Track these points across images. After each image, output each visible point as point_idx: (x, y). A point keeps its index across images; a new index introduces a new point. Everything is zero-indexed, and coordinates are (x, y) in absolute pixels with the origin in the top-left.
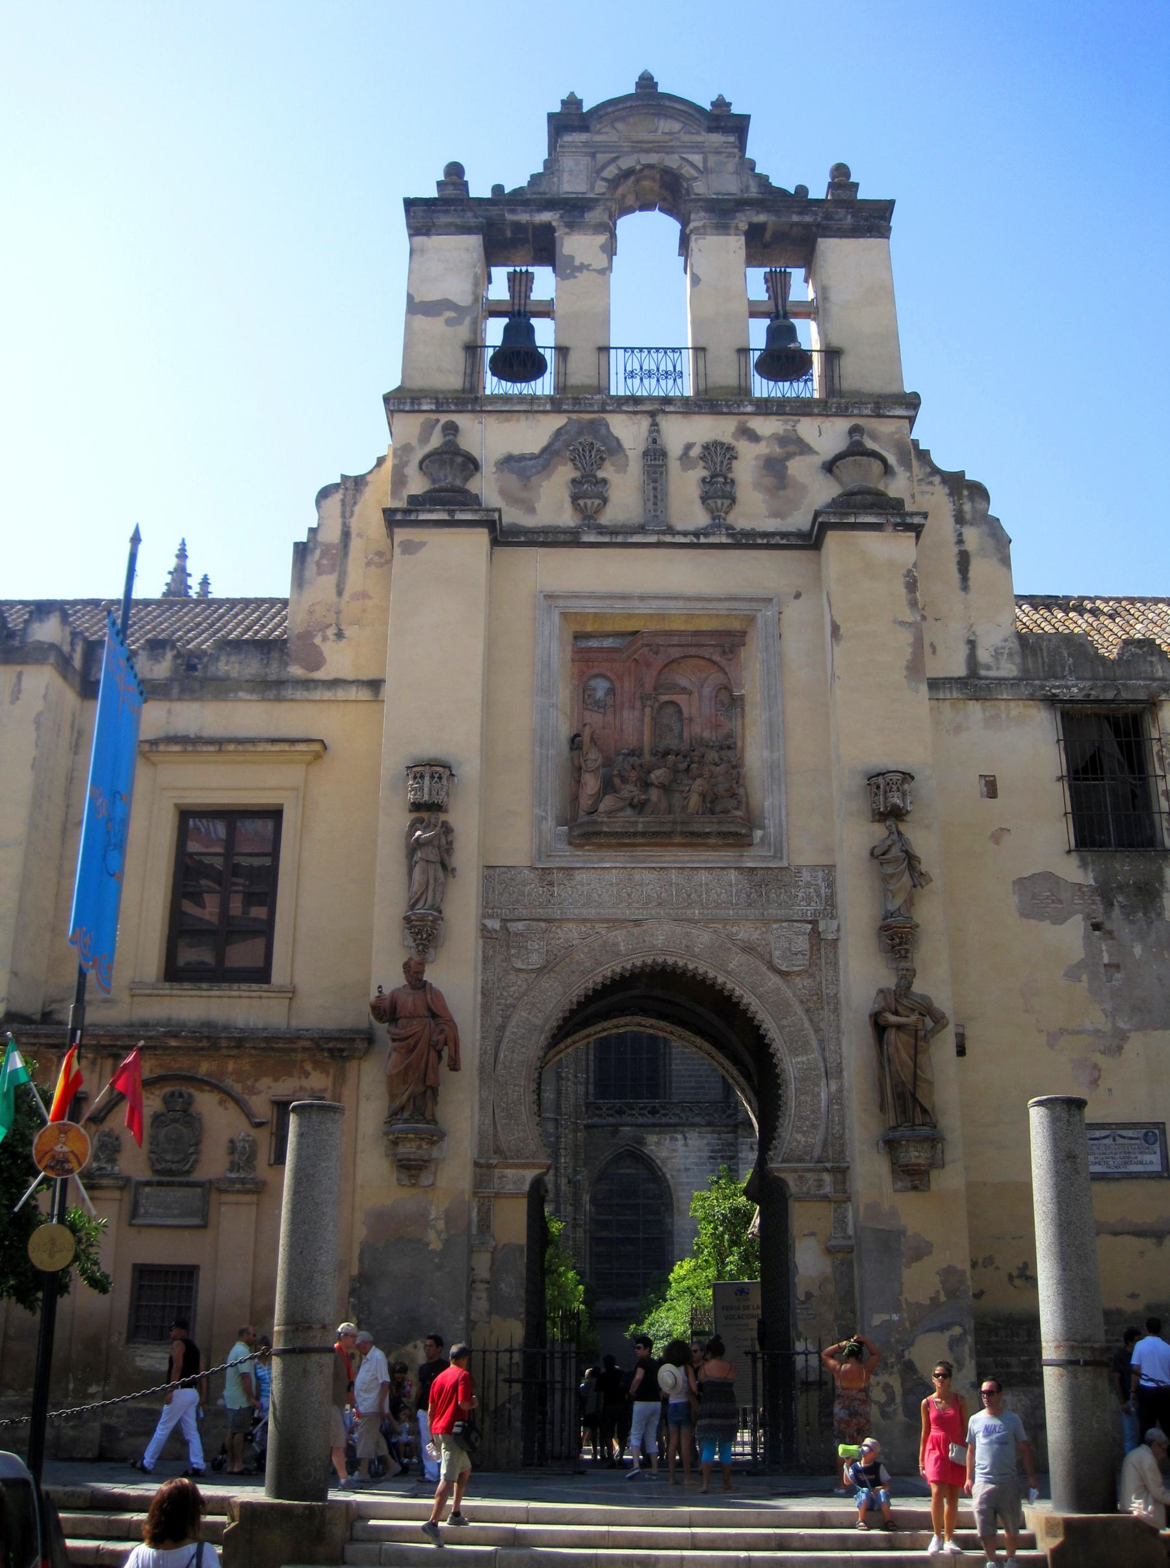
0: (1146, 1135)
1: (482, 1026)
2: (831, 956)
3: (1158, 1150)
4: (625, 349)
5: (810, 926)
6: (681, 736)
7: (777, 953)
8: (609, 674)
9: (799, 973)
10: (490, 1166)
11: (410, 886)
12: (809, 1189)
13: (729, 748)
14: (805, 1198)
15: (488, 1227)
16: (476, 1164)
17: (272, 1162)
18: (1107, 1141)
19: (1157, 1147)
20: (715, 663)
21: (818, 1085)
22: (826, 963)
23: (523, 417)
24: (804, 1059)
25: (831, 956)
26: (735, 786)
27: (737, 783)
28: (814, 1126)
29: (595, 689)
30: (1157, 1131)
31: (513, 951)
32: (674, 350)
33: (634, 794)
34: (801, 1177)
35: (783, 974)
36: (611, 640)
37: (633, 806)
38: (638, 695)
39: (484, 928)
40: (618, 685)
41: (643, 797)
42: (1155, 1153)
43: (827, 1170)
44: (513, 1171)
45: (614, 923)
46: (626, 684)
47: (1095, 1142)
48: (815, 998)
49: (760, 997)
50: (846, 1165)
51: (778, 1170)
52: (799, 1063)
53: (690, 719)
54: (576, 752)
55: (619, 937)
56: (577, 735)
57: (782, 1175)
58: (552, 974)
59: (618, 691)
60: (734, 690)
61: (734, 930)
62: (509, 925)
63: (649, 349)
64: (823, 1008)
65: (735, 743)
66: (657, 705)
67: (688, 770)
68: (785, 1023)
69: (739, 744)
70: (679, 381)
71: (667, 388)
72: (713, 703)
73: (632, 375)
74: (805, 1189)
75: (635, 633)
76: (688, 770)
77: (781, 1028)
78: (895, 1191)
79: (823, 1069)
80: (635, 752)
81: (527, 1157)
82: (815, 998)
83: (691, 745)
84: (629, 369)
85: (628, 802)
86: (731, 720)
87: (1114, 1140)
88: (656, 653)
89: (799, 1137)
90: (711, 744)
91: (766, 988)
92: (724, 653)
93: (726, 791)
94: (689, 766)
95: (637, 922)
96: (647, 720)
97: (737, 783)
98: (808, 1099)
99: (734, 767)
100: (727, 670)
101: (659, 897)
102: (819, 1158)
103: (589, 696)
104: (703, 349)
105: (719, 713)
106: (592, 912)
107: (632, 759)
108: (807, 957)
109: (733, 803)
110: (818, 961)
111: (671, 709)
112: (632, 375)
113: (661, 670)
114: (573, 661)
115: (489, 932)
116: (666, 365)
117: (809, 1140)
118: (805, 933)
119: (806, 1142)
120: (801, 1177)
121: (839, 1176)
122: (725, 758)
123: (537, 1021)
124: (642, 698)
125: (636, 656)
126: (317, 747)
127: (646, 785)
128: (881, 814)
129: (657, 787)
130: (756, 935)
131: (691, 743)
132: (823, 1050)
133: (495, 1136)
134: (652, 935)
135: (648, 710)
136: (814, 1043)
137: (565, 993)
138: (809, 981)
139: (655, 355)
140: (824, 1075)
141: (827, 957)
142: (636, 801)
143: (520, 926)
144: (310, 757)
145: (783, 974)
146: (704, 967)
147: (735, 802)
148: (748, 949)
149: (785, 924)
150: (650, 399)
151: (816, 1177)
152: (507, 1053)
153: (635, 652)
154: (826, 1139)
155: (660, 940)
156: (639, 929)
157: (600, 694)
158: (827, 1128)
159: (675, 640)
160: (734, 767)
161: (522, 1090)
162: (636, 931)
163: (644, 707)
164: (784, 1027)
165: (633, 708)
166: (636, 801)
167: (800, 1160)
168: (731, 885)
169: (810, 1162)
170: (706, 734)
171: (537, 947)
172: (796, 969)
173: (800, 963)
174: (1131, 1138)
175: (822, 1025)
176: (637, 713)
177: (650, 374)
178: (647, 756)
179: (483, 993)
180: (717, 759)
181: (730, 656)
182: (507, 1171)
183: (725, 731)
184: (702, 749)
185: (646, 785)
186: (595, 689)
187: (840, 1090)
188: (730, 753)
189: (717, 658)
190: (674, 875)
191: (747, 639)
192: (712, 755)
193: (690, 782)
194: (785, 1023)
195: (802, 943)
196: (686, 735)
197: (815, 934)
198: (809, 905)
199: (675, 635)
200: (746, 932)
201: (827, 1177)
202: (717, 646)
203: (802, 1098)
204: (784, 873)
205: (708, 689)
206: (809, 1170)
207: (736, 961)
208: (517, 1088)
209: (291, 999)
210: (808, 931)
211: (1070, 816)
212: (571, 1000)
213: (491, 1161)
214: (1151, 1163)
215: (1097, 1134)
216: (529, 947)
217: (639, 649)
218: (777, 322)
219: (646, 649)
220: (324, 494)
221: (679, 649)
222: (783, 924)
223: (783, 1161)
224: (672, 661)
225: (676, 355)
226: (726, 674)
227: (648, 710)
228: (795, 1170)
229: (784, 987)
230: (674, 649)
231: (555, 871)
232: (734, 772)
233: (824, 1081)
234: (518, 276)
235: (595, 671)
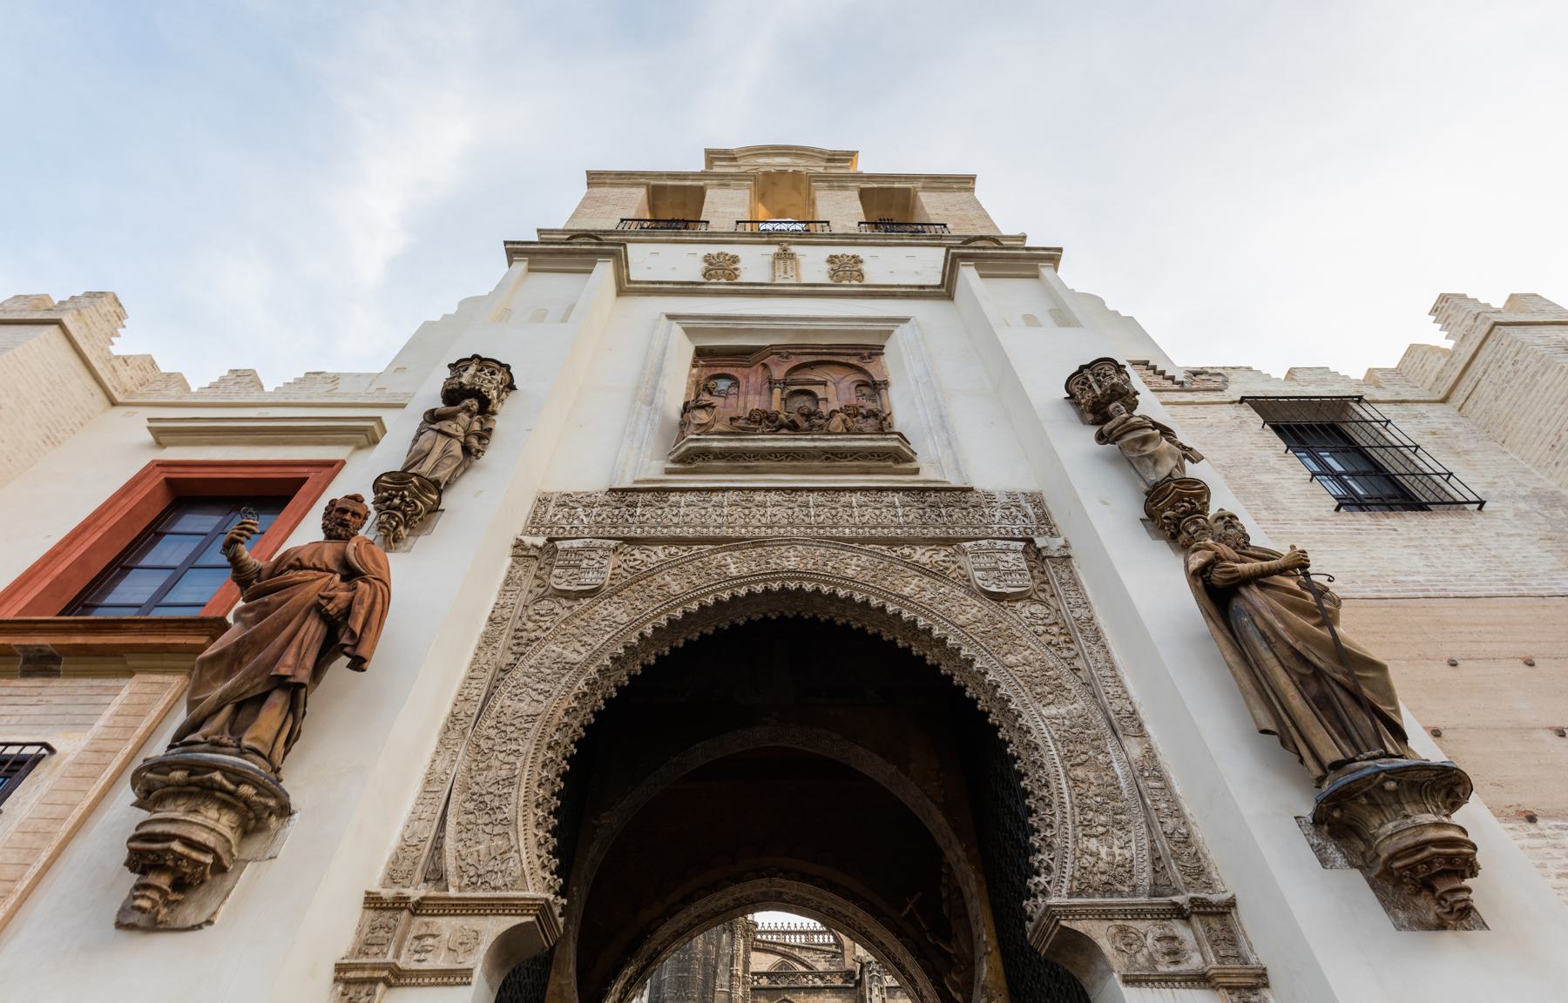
1: (475, 661)
2: (1065, 576)
5: (1023, 544)
10: (400, 903)
12: (1152, 960)
16: (373, 902)
25: (1065, 576)
31: (556, 572)
34: (1123, 931)
39: (519, 544)
43: (1179, 913)
48: (1055, 629)
51: (1071, 912)
57: (1080, 926)
58: (615, 598)
62: (557, 543)
68: (1011, 659)
74: (1141, 959)
81: (495, 888)
91: (969, 616)
95: (757, 543)
98: (1091, 775)
104: (828, 222)
106: (689, 532)
110: (1046, 587)
115: (526, 549)
117: (1117, 851)
118: (1015, 551)
120: (1123, 931)
121: (1215, 924)
123: (573, 657)
134: (780, 557)
140: (1109, 732)
143: (577, 544)
151: (1158, 932)
152: (508, 702)
156: (759, 550)
161: (522, 758)
167: (1108, 889)
171: (597, 565)
175: (1079, 663)
179: (491, 619)
182: (442, 922)
187: (1150, 754)
189: (854, 361)
194: (1011, 659)
195: (1014, 558)
198: (1014, 523)
204: (969, 494)
206: (1139, 914)
207: (911, 586)
208: (512, 758)
210: (1021, 549)
212: (641, 634)
213: (409, 892)
216: (584, 565)
222: (980, 542)
223: (1070, 895)
228: (1105, 914)
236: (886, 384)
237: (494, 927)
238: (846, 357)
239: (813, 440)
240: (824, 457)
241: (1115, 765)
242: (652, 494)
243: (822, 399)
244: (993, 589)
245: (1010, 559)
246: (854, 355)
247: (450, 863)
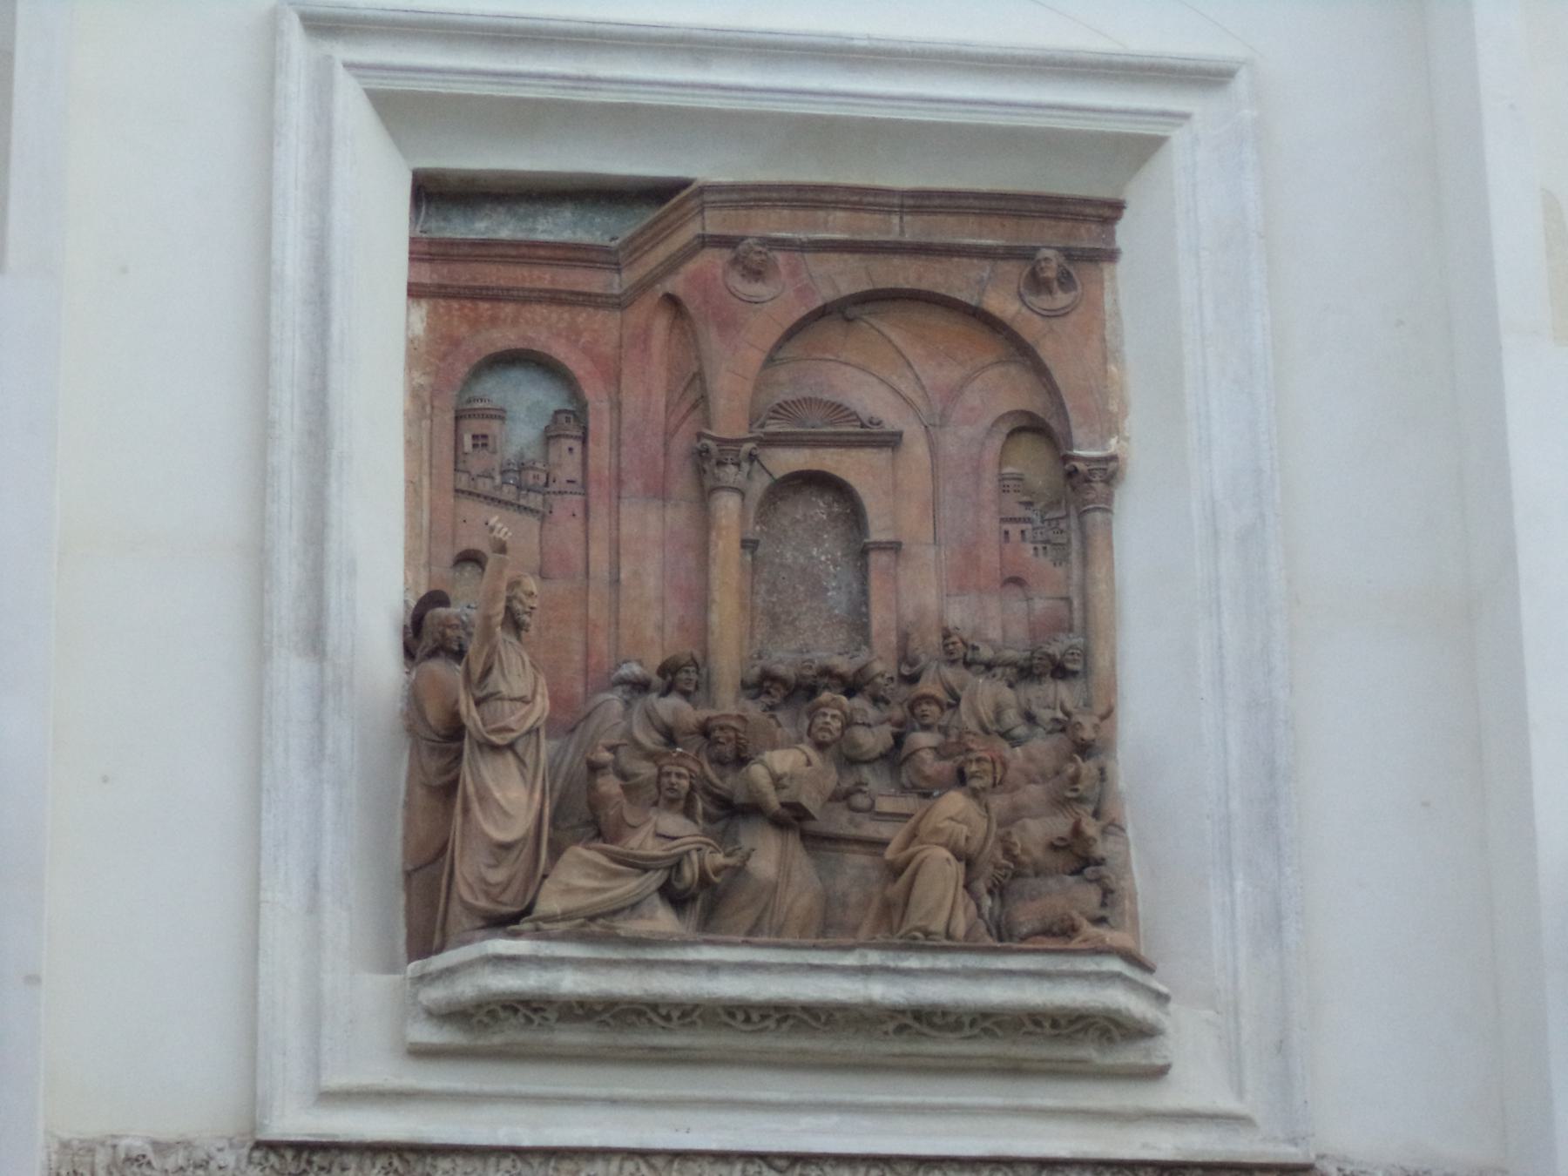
6: (859, 626)
8: (559, 351)
13: (1060, 671)
26: (1091, 828)
27: (1096, 814)
29: (500, 415)
33: (677, 848)
36: (567, 214)
37: (675, 898)
38: (682, 443)
41: (720, 859)
54: (438, 667)
56: (436, 598)
59: (600, 422)
60: (1079, 435)
65: (1085, 654)
66: (760, 484)
67: (895, 756)
69: (1101, 662)
72: (989, 484)
75: (659, 193)
76: (895, 756)
80: (671, 676)
83: (905, 656)
85: (655, 879)
86: (1062, 559)
88: (756, 274)
90: (986, 653)
92: (1037, 283)
93: (1053, 847)
94: (899, 740)
96: (726, 545)
97: (1096, 814)
100: (1047, 352)
105: (1014, 529)
107: (669, 707)
109: (1090, 896)
111: (819, 508)
113: (778, 346)
114: (415, 292)
122: (1045, 715)
124: (703, 454)
125: (675, 285)
131: (904, 637)
142: (689, 873)
147: (1092, 895)
153: (672, 265)
159: (837, 226)
160: (1084, 749)
163: (706, 493)
165: (659, 492)
166: (689, 873)
170: (958, 615)
176: (679, 516)
180: (1011, 717)
181: (1061, 299)
183: (1040, 605)
184: (952, 675)
188: (1063, 692)
189: (1003, 304)
191: (1126, 233)
193: (908, 804)
196: (880, 617)
199: (835, 205)
202: (1010, 254)
205: (966, 431)
217: (688, 253)
219: (714, 260)
221: (853, 261)
224: (822, 313)
226: (1040, 370)
227: (728, 506)
230: (834, 261)
231: (351, 1160)
232: (1088, 767)
235: (505, 338)
236: (1109, 471)
238: (982, 269)
239: (866, 971)
240: (891, 1026)
242: (382, 1161)
243: (882, 547)
246: (1010, 254)
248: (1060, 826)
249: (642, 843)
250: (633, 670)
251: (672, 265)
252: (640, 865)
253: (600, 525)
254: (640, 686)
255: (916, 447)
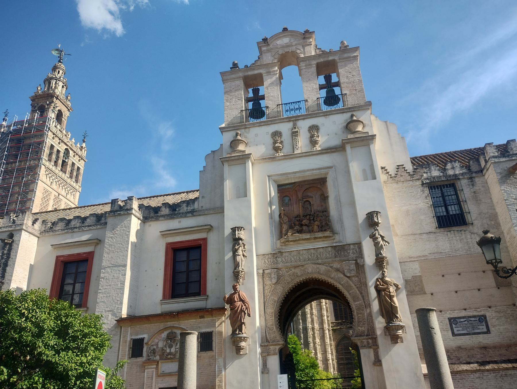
0: (479, 319)
2: (362, 270)
3: (485, 325)
4: (285, 104)
5: (355, 261)
7: (346, 271)
9: (353, 276)
10: (265, 346)
11: (234, 263)
13: (325, 211)
14: (364, 347)
15: (266, 366)
17: (199, 351)
18: (466, 322)
19: (484, 323)
20: (319, 188)
21: (363, 310)
22: (361, 272)
23: (258, 127)
24: (358, 303)
26: (328, 222)
28: (364, 324)
30: (483, 318)
32: (298, 102)
35: (348, 277)
36: (288, 186)
40: (291, 198)
42: (483, 325)
43: (370, 338)
44: (273, 347)
45: (295, 267)
46: (294, 198)
47: (462, 323)
49: (342, 285)
50: (376, 336)
52: (356, 304)
53: (313, 205)
55: (298, 271)
57: (356, 341)
59: (292, 200)
60: (325, 194)
61: (332, 265)
63: (291, 103)
64: (362, 286)
65: (327, 210)
66: (303, 202)
67: (313, 219)
68: (351, 292)
69: (328, 210)
70: (300, 110)
71: (298, 113)
73: (287, 111)
75: (294, 183)
76: (313, 219)
77: (350, 294)
78: (392, 343)
79: (364, 306)
82: (359, 283)
84: (286, 109)
85: (296, 231)
87: (468, 322)
89: (359, 328)
92: (321, 185)
99: (327, 217)
101: (308, 258)
102: (367, 334)
103: (284, 202)
108: (355, 271)
111: (308, 203)
112: (287, 111)
114: (278, 193)
116: (297, 106)
117: (363, 329)
118: (353, 264)
119: (362, 329)
123: (275, 299)
125: (296, 189)
126: (209, 227)
127: (302, 225)
128: (371, 225)
129: (305, 226)
130: (339, 266)
132: (364, 299)
133: (266, 335)
135: (300, 204)
136: (360, 297)
137: (283, 290)
138: (357, 278)
139: (293, 104)
141: (361, 270)
142: (299, 230)
144: (207, 230)
145: (348, 277)
146: (323, 278)
148: (338, 270)
149: (347, 262)
150: (293, 117)
153: (295, 188)
154: (368, 329)
155: (310, 270)
157: (287, 201)
158: (368, 324)
162: (303, 268)
164: (350, 293)
167: (361, 336)
168: (329, 252)
169: (364, 336)
170: (318, 209)
172: (352, 275)
173: (353, 273)
174: (474, 321)
176: (298, 205)
177: (292, 110)
178: (302, 217)
185: (302, 225)
186: (285, 200)
189: (319, 186)
190: (312, 251)
192: (321, 214)
194: (351, 292)
195: (353, 267)
197: (357, 264)
200: (336, 265)
201: (370, 341)
203: (359, 315)
206: (364, 339)
209: (206, 300)
210: (354, 263)
211: (435, 218)
214: (483, 329)
215: (462, 320)
218: (328, 89)
220: (207, 156)
225: (299, 103)
227: (300, 204)
228: (359, 340)
229: (349, 281)
233: (365, 309)
234: (255, 90)
235: (285, 195)
236: (328, 197)
237: (278, 348)
241: (365, 313)
244: (348, 275)
245: (352, 266)
247: (269, 339)
248: (325, 223)
249: (295, 228)
250: (295, 216)
251: (295, 188)
252: (295, 230)
253: (292, 207)
254: (296, 217)
255: (314, 198)
